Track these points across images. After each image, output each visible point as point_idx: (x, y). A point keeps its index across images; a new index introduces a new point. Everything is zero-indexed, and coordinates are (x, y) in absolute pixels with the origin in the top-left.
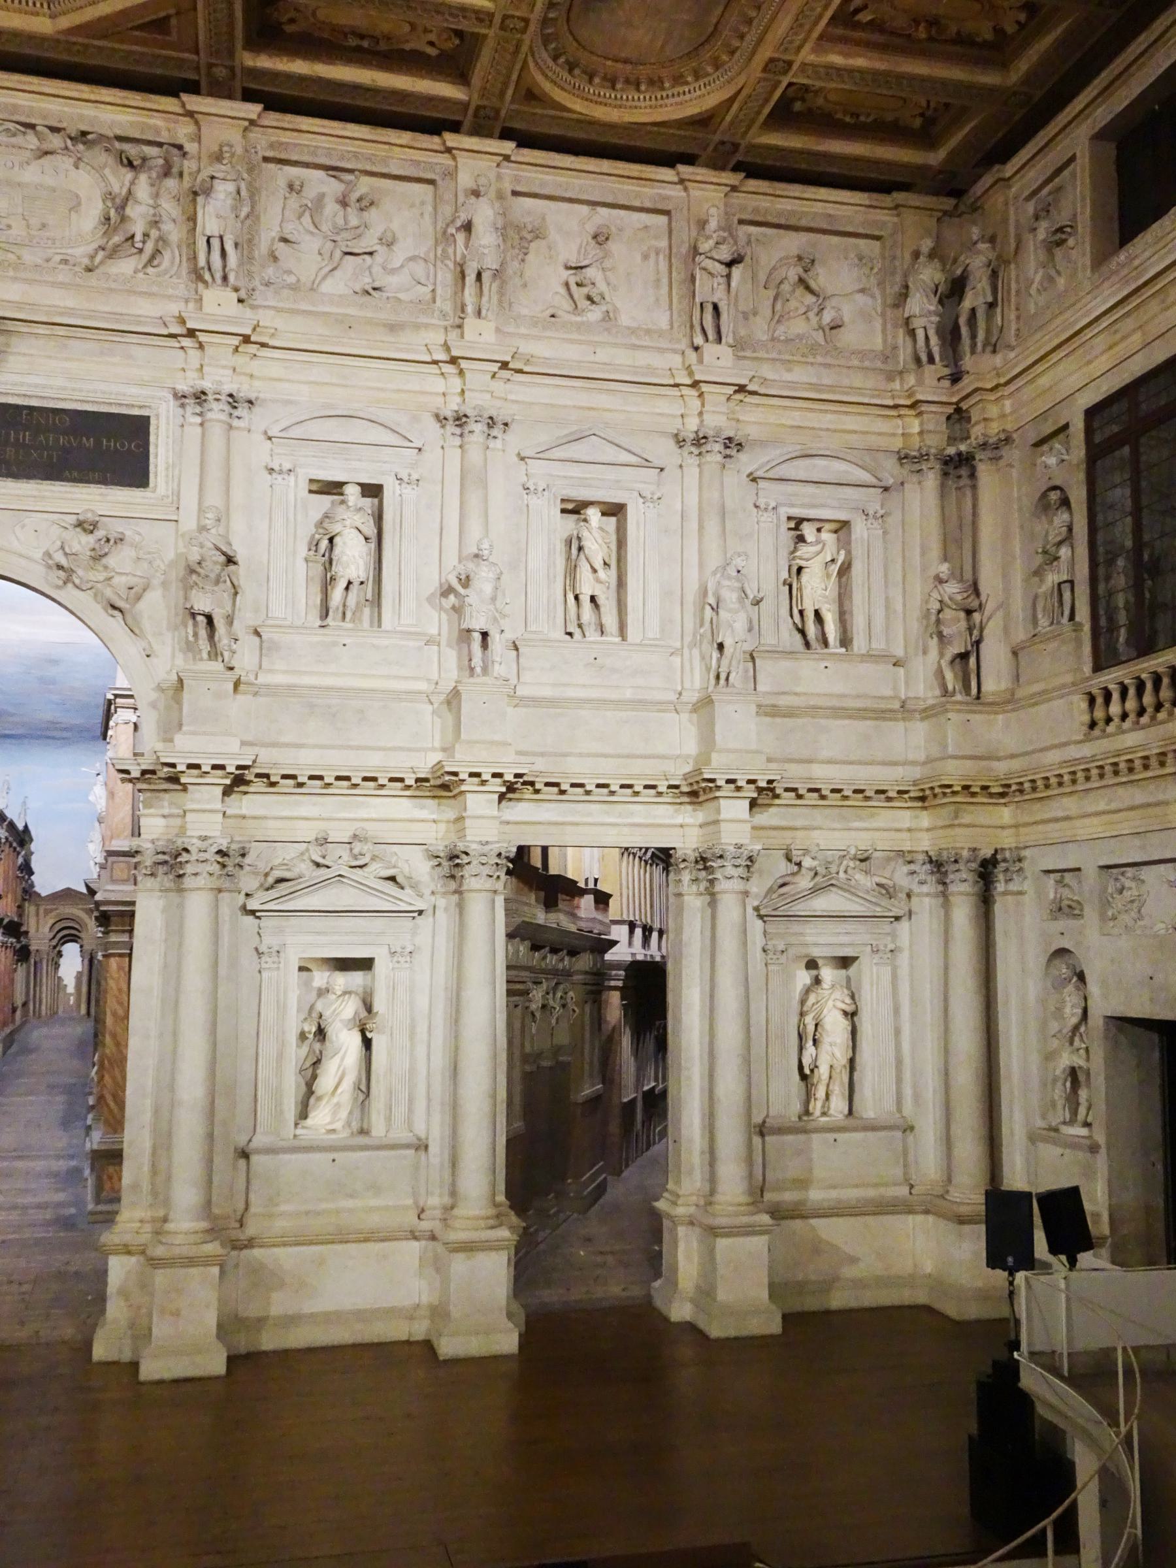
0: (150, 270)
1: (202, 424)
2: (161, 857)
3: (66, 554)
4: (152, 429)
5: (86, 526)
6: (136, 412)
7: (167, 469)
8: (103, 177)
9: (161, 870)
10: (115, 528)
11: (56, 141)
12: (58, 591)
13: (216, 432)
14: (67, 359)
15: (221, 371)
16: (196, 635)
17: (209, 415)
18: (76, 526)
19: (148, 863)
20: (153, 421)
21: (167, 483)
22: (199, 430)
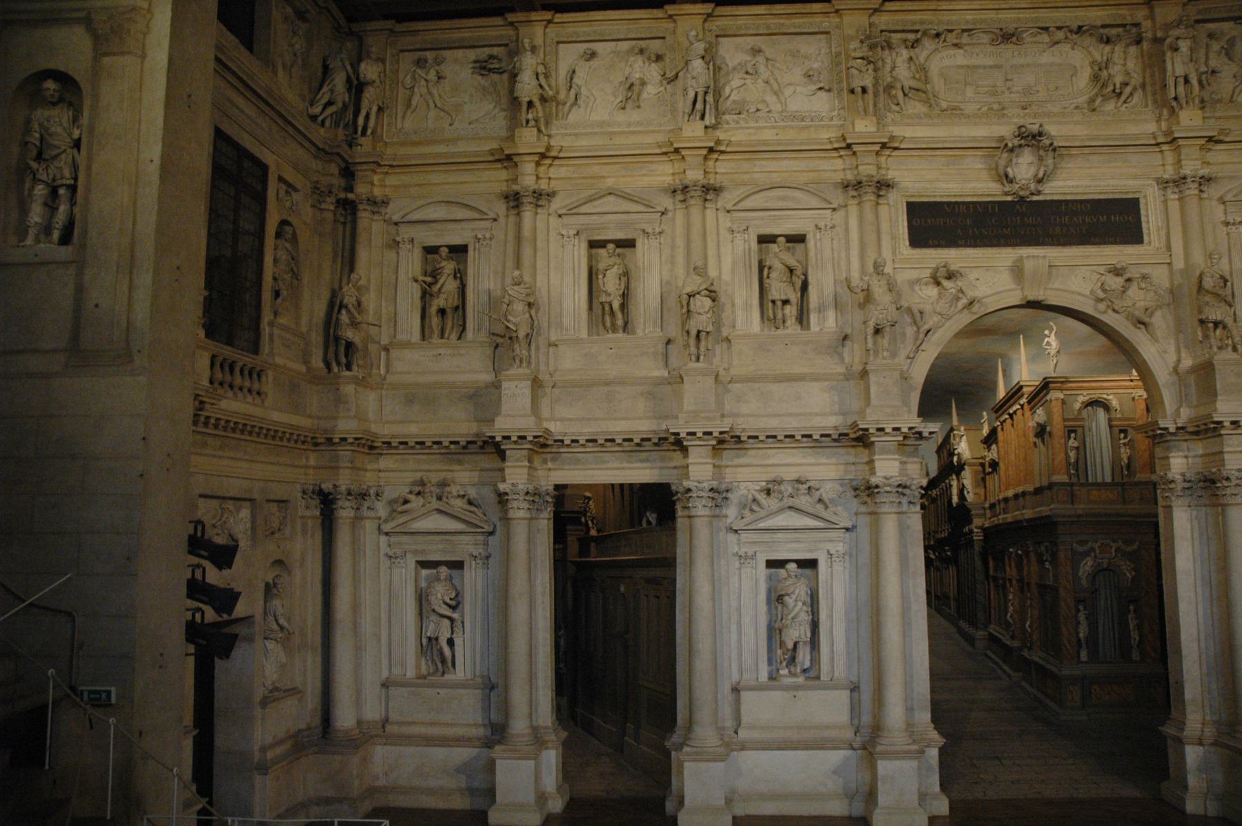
0: (1126, 105)
1: (1179, 199)
2: (1186, 485)
3: (1104, 291)
4: (1142, 206)
5: (1117, 271)
6: (1130, 196)
7: (1158, 230)
8: (1090, 53)
9: (1188, 492)
10: (1134, 273)
11: (1060, 35)
12: (1104, 315)
13: (1192, 205)
14: (1089, 168)
15: (1193, 163)
16: (1206, 337)
17: (1188, 192)
18: (1110, 272)
19: (1179, 487)
20: (1142, 201)
21: (1159, 239)
22: (1177, 203)
